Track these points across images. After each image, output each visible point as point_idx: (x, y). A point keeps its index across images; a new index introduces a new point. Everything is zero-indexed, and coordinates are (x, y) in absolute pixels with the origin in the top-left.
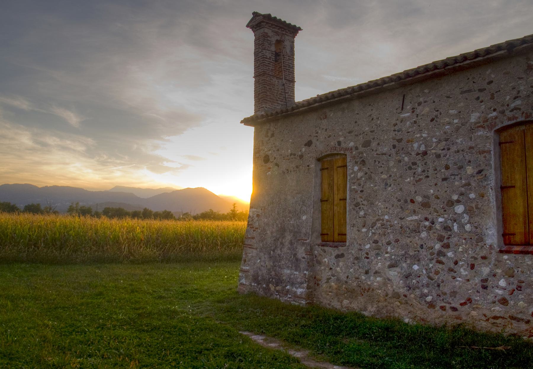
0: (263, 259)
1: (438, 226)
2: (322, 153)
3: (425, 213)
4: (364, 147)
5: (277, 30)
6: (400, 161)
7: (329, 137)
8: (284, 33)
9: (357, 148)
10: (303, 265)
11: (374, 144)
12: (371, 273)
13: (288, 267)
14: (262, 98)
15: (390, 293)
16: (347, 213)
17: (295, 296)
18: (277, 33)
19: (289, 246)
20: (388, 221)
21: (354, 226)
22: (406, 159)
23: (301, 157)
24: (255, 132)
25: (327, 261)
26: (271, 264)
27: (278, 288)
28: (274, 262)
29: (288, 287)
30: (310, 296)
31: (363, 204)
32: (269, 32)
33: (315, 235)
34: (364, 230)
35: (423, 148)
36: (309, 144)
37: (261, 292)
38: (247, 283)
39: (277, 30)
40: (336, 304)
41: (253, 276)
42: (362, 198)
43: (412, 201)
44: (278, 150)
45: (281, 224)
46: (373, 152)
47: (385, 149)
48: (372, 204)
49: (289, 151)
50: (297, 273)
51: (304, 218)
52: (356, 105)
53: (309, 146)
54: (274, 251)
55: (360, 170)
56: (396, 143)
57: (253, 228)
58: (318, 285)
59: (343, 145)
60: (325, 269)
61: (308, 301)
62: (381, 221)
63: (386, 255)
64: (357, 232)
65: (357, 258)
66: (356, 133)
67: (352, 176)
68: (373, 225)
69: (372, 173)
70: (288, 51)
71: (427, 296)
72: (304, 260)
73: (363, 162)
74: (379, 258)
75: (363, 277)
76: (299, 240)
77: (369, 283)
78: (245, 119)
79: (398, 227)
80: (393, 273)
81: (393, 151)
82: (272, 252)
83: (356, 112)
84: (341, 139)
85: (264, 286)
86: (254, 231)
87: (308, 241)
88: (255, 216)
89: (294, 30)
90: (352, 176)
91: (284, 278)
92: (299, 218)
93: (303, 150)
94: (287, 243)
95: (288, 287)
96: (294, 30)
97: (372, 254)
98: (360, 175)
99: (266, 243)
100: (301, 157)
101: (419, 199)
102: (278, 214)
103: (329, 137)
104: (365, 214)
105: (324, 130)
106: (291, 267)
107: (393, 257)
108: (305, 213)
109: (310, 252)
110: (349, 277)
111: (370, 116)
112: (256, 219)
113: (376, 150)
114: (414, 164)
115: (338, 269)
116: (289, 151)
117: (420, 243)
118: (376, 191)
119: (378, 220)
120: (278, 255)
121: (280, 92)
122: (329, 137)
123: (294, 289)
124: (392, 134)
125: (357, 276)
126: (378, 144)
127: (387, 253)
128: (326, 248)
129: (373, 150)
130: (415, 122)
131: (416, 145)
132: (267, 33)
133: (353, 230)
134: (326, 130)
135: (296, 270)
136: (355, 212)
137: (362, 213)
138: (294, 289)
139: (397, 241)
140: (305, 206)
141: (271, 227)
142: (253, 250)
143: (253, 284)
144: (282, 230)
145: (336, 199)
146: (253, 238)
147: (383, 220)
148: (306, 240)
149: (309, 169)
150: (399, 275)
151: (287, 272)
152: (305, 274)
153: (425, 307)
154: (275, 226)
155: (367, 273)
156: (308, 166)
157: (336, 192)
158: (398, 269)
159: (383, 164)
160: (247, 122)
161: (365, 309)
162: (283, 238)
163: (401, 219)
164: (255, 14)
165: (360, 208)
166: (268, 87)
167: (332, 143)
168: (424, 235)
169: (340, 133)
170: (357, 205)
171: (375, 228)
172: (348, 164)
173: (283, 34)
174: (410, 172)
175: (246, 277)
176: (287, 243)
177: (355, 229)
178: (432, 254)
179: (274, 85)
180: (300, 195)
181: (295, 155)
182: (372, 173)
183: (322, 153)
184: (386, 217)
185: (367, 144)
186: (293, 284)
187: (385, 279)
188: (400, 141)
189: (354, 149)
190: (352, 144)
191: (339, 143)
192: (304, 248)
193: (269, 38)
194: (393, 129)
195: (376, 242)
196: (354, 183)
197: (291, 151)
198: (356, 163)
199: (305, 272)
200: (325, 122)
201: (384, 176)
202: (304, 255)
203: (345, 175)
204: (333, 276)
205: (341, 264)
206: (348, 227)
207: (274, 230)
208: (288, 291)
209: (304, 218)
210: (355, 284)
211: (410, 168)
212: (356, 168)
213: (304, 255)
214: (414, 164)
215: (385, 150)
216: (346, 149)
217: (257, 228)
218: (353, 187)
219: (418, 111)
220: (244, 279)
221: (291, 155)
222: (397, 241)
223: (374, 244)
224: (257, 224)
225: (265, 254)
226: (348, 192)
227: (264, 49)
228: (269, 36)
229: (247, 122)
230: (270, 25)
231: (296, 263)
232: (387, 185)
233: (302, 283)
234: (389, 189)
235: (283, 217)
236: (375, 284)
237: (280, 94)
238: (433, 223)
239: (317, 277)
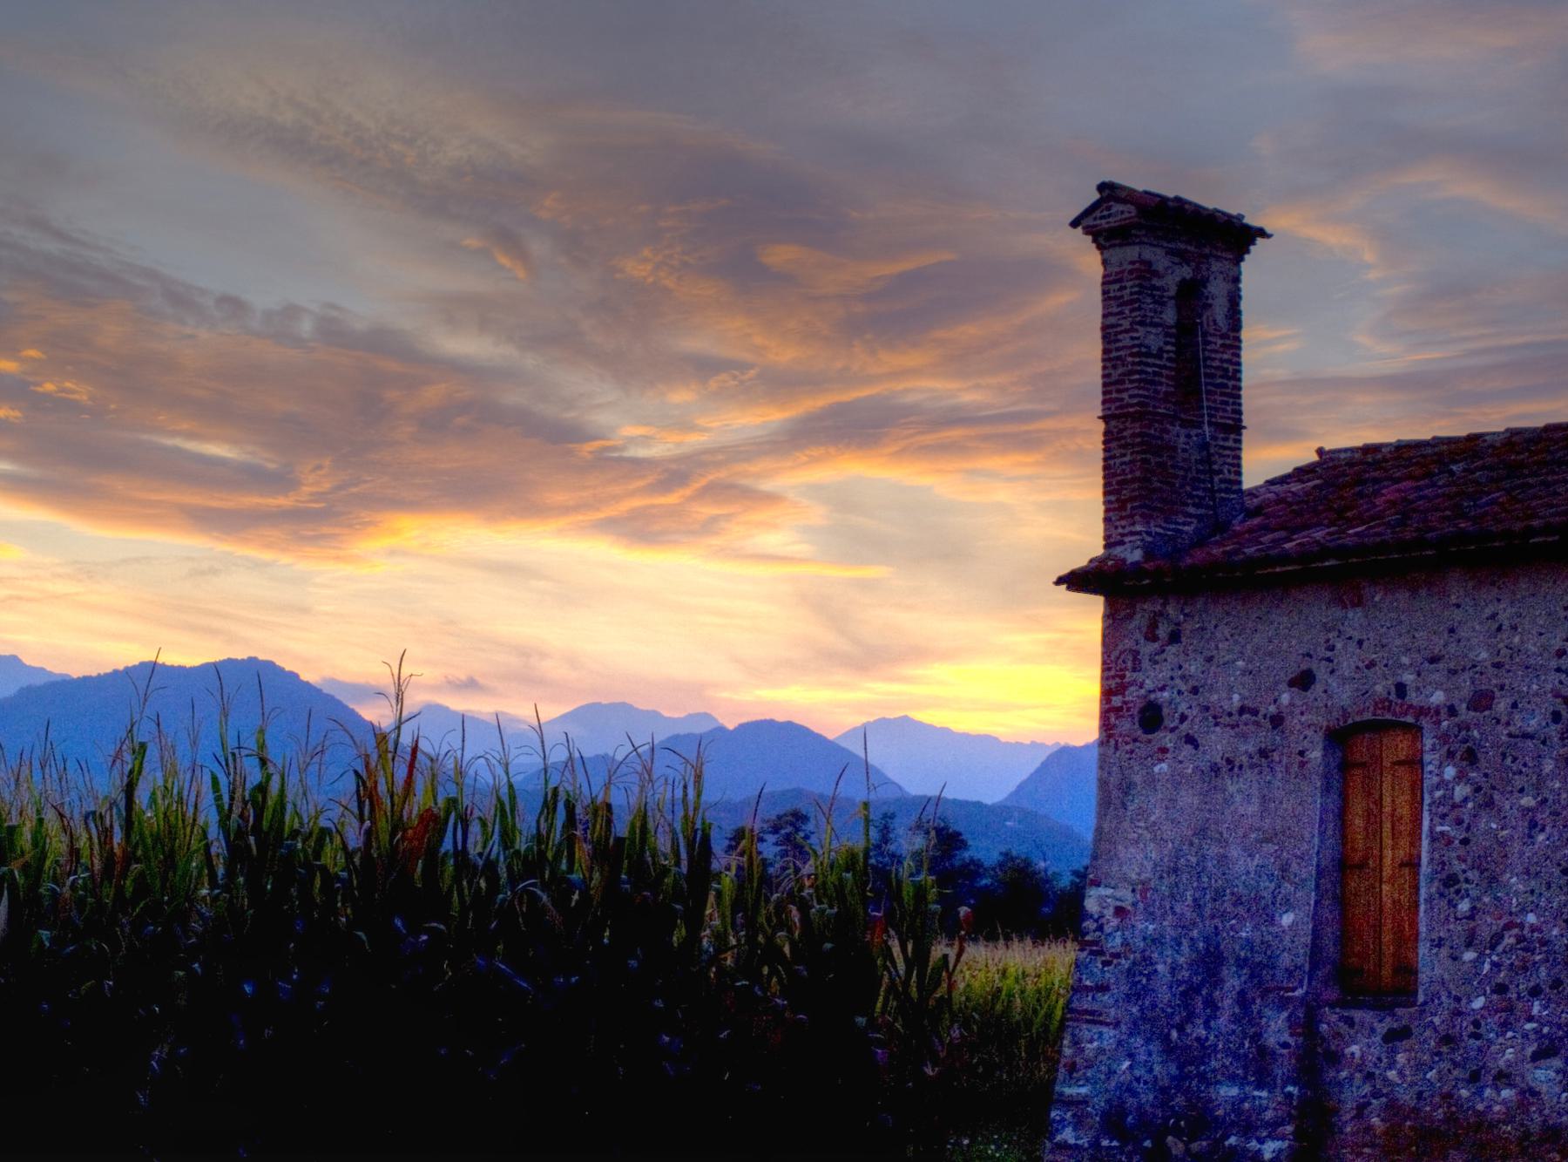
2: (1345, 713)
4: (1475, 710)
7: (1371, 665)
9: (1452, 711)
11: (1502, 706)
13: (1233, 1078)
15: (1535, 1127)
16: (1422, 908)
19: (1237, 1010)
20: (1533, 929)
21: (1439, 943)
23: (1277, 721)
24: (1106, 617)
25: (1358, 1055)
26: (1173, 1070)
28: (1180, 1067)
29: (1233, 1140)
31: (1467, 881)
34: (1469, 956)
36: (1304, 681)
38: (1084, 1142)
41: (1105, 1115)
42: (1465, 861)
45: (1207, 939)
46: (1500, 728)
47: (1533, 722)
48: (1493, 879)
49: (1236, 697)
50: (1264, 1094)
51: (1287, 919)
53: (1305, 688)
54: (1181, 1029)
55: (1461, 777)
57: (1101, 953)
59: (1413, 698)
60: (1351, 1078)
62: (1516, 931)
63: (1529, 1026)
65: (1447, 1039)
66: (1452, 665)
67: (1438, 794)
68: (1497, 938)
69: (1493, 788)
72: (1285, 1051)
73: (1471, 757)
74: (1510, 1034)
75: (1464, 1093)
77: (1480, 1107)
81: (1554, 731)
82: (1174, 1034)
83: (1453, 599)
84: (1408, 678)
86: (1105, 963)
87: (1299, 992)
88: (1109, 913)
90: (1438, 794)
91: (1220, 1112)
92: (1271, 920)
93: (1285, 698)
98: (1461, 791)
99: (1154, 1006)
100: (1277, 721)
102: (1197, 905)
103: (1368, 667)
104: (1473, 908)
106: (1245, 1078)
107: (1546, 1030)
108: (1288, 905)
109: (1306, 1025)
110: (1426, 1095)
111: (1493, 616)
112: (1115, 922)
113: (1508, 724)
115: (1392, 1074)
116: (1236, 697)
118: (1502, 844)
119: (1508, 927)
120: (1198, 1039)
122: (1368, 667)
123: (1254, 1145)
125: (1445, 1089)
126: (1515, 705)
127: (1530, 1019)
128: (1357, 1015)
134: (1360, 643)
135: (1259, 1087)
136: (1444, 903)
137: (1464, 906)
138: (1254, 1145)
142: (1105, 1029)
143: (1105, 1143)
144: (1210, 962)
145: (1388, 861)
146: (1104, 988)
147: (1521, 926)
148: (1294, 990)
149: (1302, 765)
150: (1560, 1077)
151: (1229, 1091)
152: (1290, 1095)
155: (1474, 1077)
156: (1301, 753)
157: (1388, 841)
159: (1525, 765)
167: (1379, 688)
169: (1405, 660)
170: (1451, 881)
171: (1500, 949)
172: (1427, 758)
175: (1078, 1124)
176: (1228, 1004)
177: (1444, 952)
180: (1271, 848)
181: (1255, 712)
182: (1493, 788)
183: (1345, 713)
184: (1531, 918)
185: (1481, 701)
187: (1522, 1092)
189: (1444, 711)
190: (1438, 698)
191: (1401, 689)
192: (1285, 1014)
194: (1554, 664)
195: (1501, 989)
196: (1444, 816)
197: (1243, 698)
198: (1451, 754)
199: (1290, 1088)
200: (1355, 616)
201: (1527, 801)
202: (1286, 1037)
203: (1417, 787)
204: (1376, 1094)
205: (1401, 1058)
206: (1423, 949)
207: (1182, 960)
209: (1287, 919)
210: (1440, 1114)
212: (1450, 772)
213: (1286, 1037)
215: (1533, 724)
216: (1422, 711)
217: (1117, 956)
218: (1439, 829)
221: (1242, 710)
223: (1495, 997)
224: (1118, 941)
225: (1148, 1041)
226: (1425, 843)
231: (1259, 1067)
232: (1535, 825)
234: (1541, 837)
235: (1213, 917)
236: (1497, 1108)
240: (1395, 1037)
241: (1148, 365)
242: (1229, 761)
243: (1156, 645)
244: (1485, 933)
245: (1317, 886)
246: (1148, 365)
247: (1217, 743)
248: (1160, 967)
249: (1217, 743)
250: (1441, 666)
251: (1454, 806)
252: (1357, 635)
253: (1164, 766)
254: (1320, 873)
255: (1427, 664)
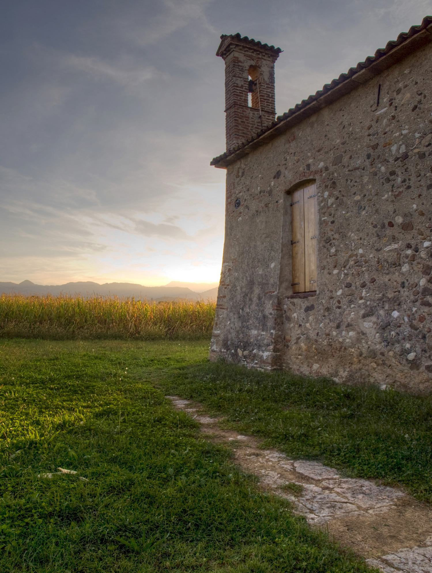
0: (232, 320)
1: (423, 254)
3: (408, 237)
5: (251, 54)
6: (375, 174)
8: (260, 56)
9: (327, 169)
10: (270, 323)
11: (345, 160)
12: (343, 327)
13: (256, 327)
14: (233, 133)
15: (364, 350)
17: (262, 361)
18: (251, 58)
19: (258, 301)
20: (362, 256)
22: (383, 169)
23: (270, 193)
25: (296, 317)
26: (240, 325)
27: (246, 353)
28: (242, 323)
30: (278, 360)
32: (241, 57)
33: (284, 285)
34: (335, 272)
35: (403, 149)
37: (230, 359)
39: (251, 54)
40: (305, 370)
41: (224, 340)
42: (332, 231)
43: (391, 225)
44: (248, 190)
45: (250, 277)
47: (359, 162)
49: (259, 188)
50: (264, 333)
51: (273, 265)
52: (326, 114)
55: (330, 196)
56: (371, 151)
58: (288, 346)
60: (294, 327)
61: (275, 367)
62: (354, 258)
63: (361, 302)
64: (328, 276)
65: (328, 309)
66: (326, 150)
67: (322, 204)
69: (343, 196)
70: (266, 79)
71: (408, 352)
72: (271, 316)
74: (352, 306)
75: (334, 333)
76: (267, 293)
77: (341, 340)
78: (214, 159)
79: (374, 262)
80: (368, 325)
82: (241, 311)
83: (326, 123)
84: (311, 161)
85: (233, 351)
86: (226, 288)
87: (276, 293)
89: (274, 53)
91: (252, 340)
92: (268, 266)
93: (272, 184)
94: (255, 299)
95: (255, 351)
96: (274, 53)
97: (345, 301)
98: (330, 201)
101: (399, 220)
103: (297, 162)
104: (336, 251)
105: (293, 155)
106: (259, 327)
107: (368, 303)
109: (279, 306)
110: (319, 334)
113: (348, 166)
114: (393, 173)
116: (259, 188)
117: (400, 280)
118: (347, 220)
119: (350, 257)
120: (247, 313)
121: (256, 126)
123: (261, 353)
124: (367, 140)
125: (327, 331)
126: (351, 157)
127: (361, 298)
128: (295, 300)
129: (344, 167)
130: (394, 117)
131: (394, 148)
132: (237, 58)
133: (323, 273)
135: (263, 331)
136: (325, 250)
137: (333, 250)
138: (261, 353)
139: (373, 281)
140: (274, 251)
141: (241, 282)
142: (224, 310)
143: (223, 350)
144: (251, 283)
147: (356, 255)
148: (274, 292)
150: (375, 326)
151: (254, 332)
152: (272, 333)
153: (406, 369)
154: (244, 280)
155: (338, 327)
158: (374, 319)
159: (356, 182)
160: (217, 162)
161: (336, 374)
162: (251, 293)
163: (378, 250)
164: (223, 37)
165: (331, 244)
166: (240, 120)
168: (405, 268)
169: (309, 154)
171: (347, 267)
173: (259, 58)
174: (387, 186)
176: (255, 299)
177: (326, 271)
178: (416, 293)
179: (249, 118)
182: (343, 196)
183: (291, 182)
184: (361, 251)
185: (337, 161)
186: (259, 347)
187: (358, 333)
188: (375, 147)
189: (324, 169)
191: (308, 166)
192: (271, 302)
193: (240, 64)
194: (367, 134)
195: (349, 286)
196: (324, 213)
197: (261, 187)
199: (272, 331)
200: (293, 144)
201: (357, 198)
202: (271, 311)
205: (311, 318)
208: (255, 356)
211: (388, 180)
213: (271, 311)
214: (393, 173)
218: (323, 219)
219: (396, 103)
220: (215, 345)
221: (260, 193)
222: (373, 281)
223: (346, 289)
225: (234, 314)
227: (234, 76)
228: (240, 62)
229: (217, 162)
230: (241, 47)
232: (361, 208)
233: (268, 345)
234: (364, 213)
236: (348, 340)
237: (256, 128)
238: (417, 250)
239: (288, 337)
240: (308, 309)
241: (237, 90)
242: (257, 211)
243: (239, 179)
244: (342, 261)
245: (282, 251)
246: (237, 90)
247: (254, 206)
248: (238, 288)
249: (254, 206)
250: (322, 152)
251: (328, 208)
252: (293, 151)
253: (240, 218)
254: (283, 245)
255: (317, 153)
